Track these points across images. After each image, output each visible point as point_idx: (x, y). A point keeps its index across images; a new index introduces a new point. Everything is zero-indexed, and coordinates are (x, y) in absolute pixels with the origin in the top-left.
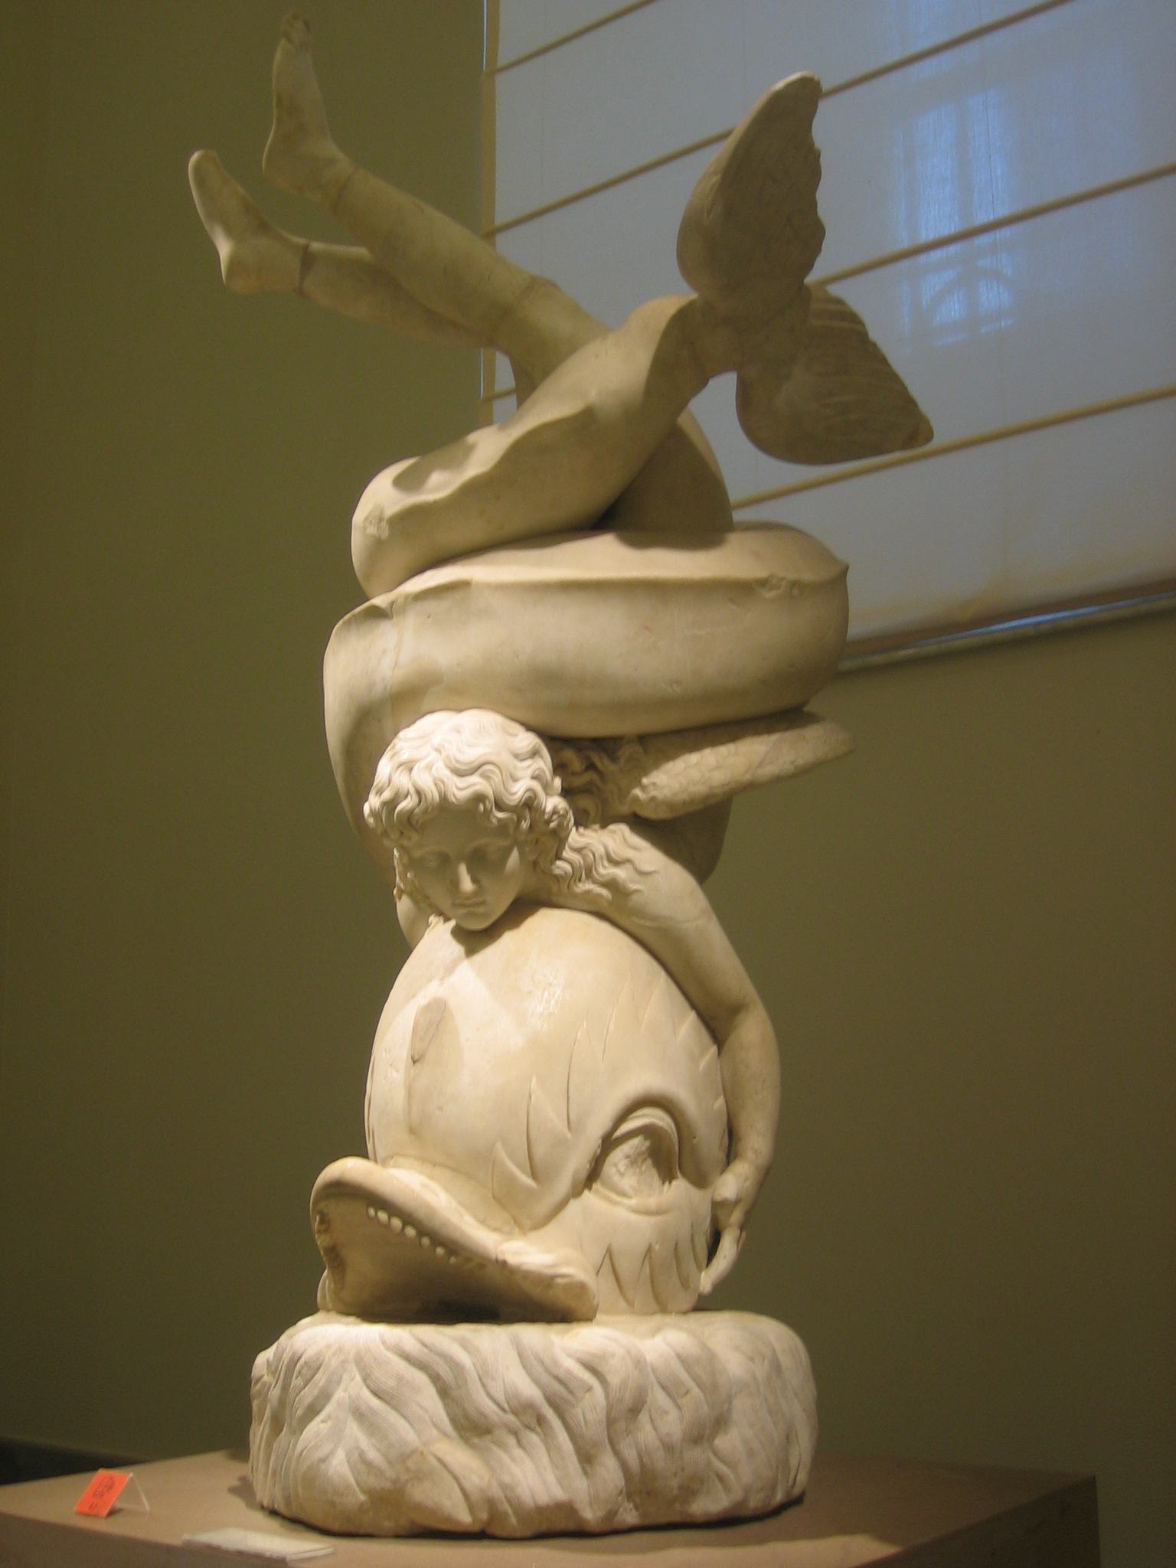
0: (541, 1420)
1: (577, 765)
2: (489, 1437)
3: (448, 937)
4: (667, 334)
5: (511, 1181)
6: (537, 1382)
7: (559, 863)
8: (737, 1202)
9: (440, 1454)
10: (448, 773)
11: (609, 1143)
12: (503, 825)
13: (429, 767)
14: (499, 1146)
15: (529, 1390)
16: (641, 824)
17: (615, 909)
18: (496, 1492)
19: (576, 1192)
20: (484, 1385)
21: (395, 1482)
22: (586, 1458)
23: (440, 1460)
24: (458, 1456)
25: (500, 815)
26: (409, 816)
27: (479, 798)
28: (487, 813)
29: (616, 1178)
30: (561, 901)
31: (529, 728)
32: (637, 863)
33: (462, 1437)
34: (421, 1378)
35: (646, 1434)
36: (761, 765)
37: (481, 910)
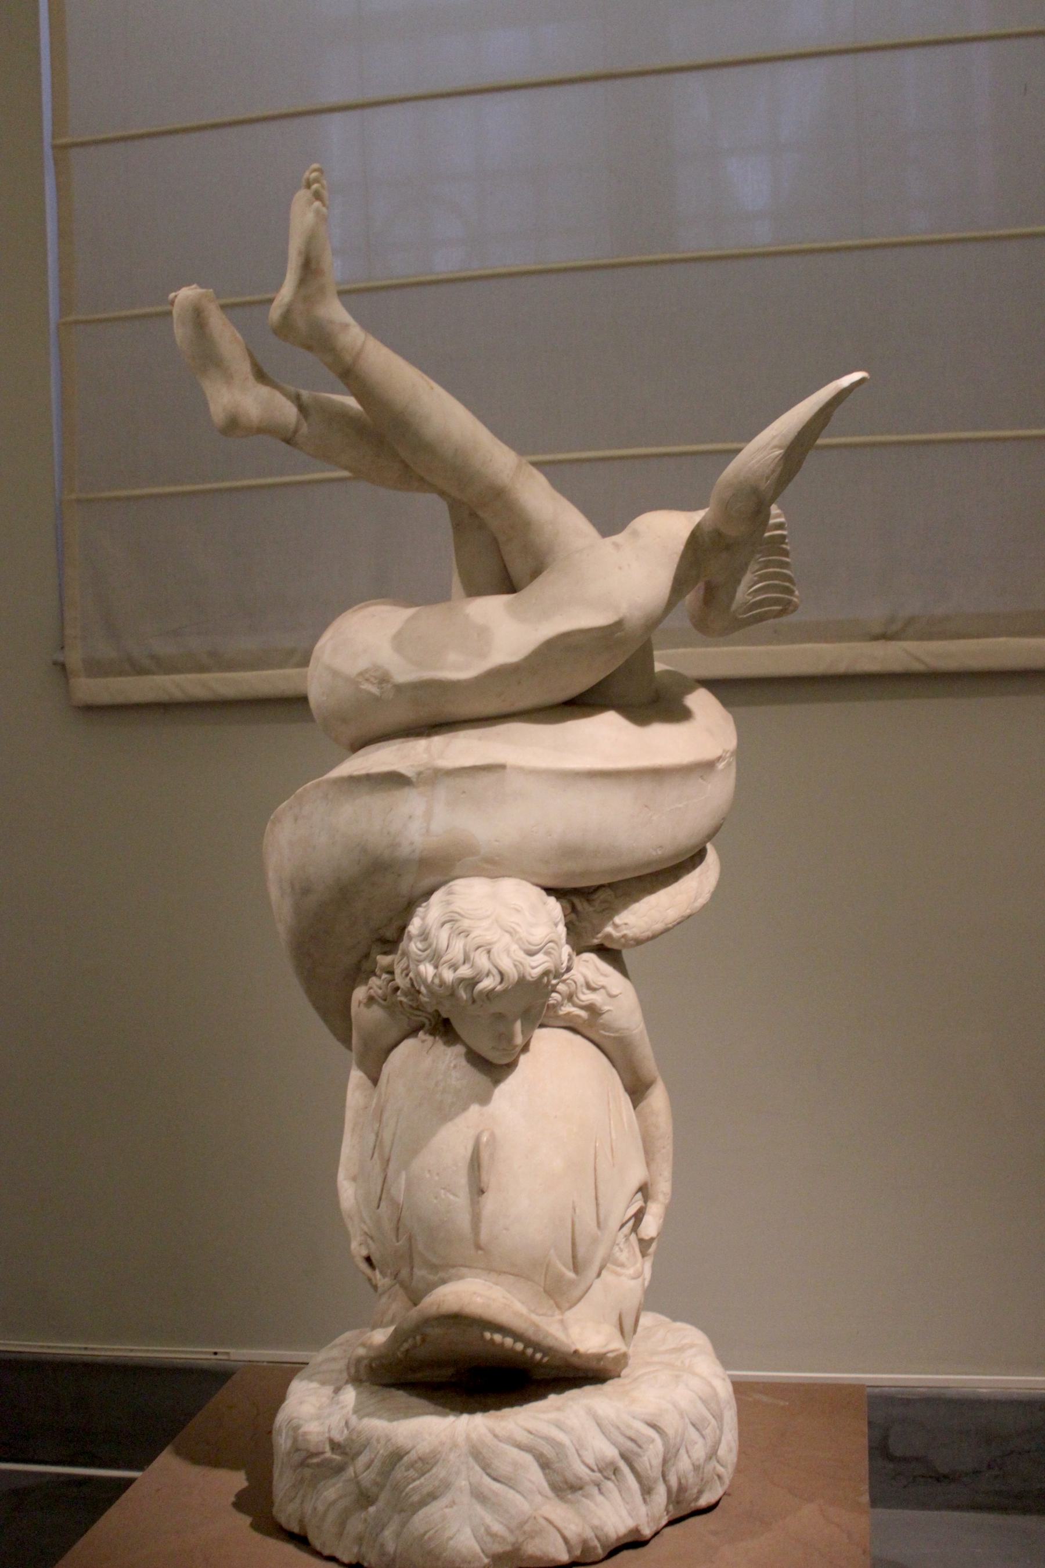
0: (616, 1471)
2: (580, 1492)
4: (683, 556)
5: (561, 1277)
6: (614, 1444)
7: (554, 995)
9: (547, 1515)
10: (522, 954)
13: (508, 952)
14: (552, 1251)
15: (611, 1452)
17: (589, 1027)
18: (589, 1534)
19: (599, 1275)
20: (579, 1456)
21: (513, 1544)
22: (647, 1491)
23: (547, 1519)
24: (557, 1511)
26: (489, 995)
29: (618, 1254)
31: (549, 891)
33: (558, 1496)
34: (528, 1458)
35: (684, 1464)
36: (696, 899)
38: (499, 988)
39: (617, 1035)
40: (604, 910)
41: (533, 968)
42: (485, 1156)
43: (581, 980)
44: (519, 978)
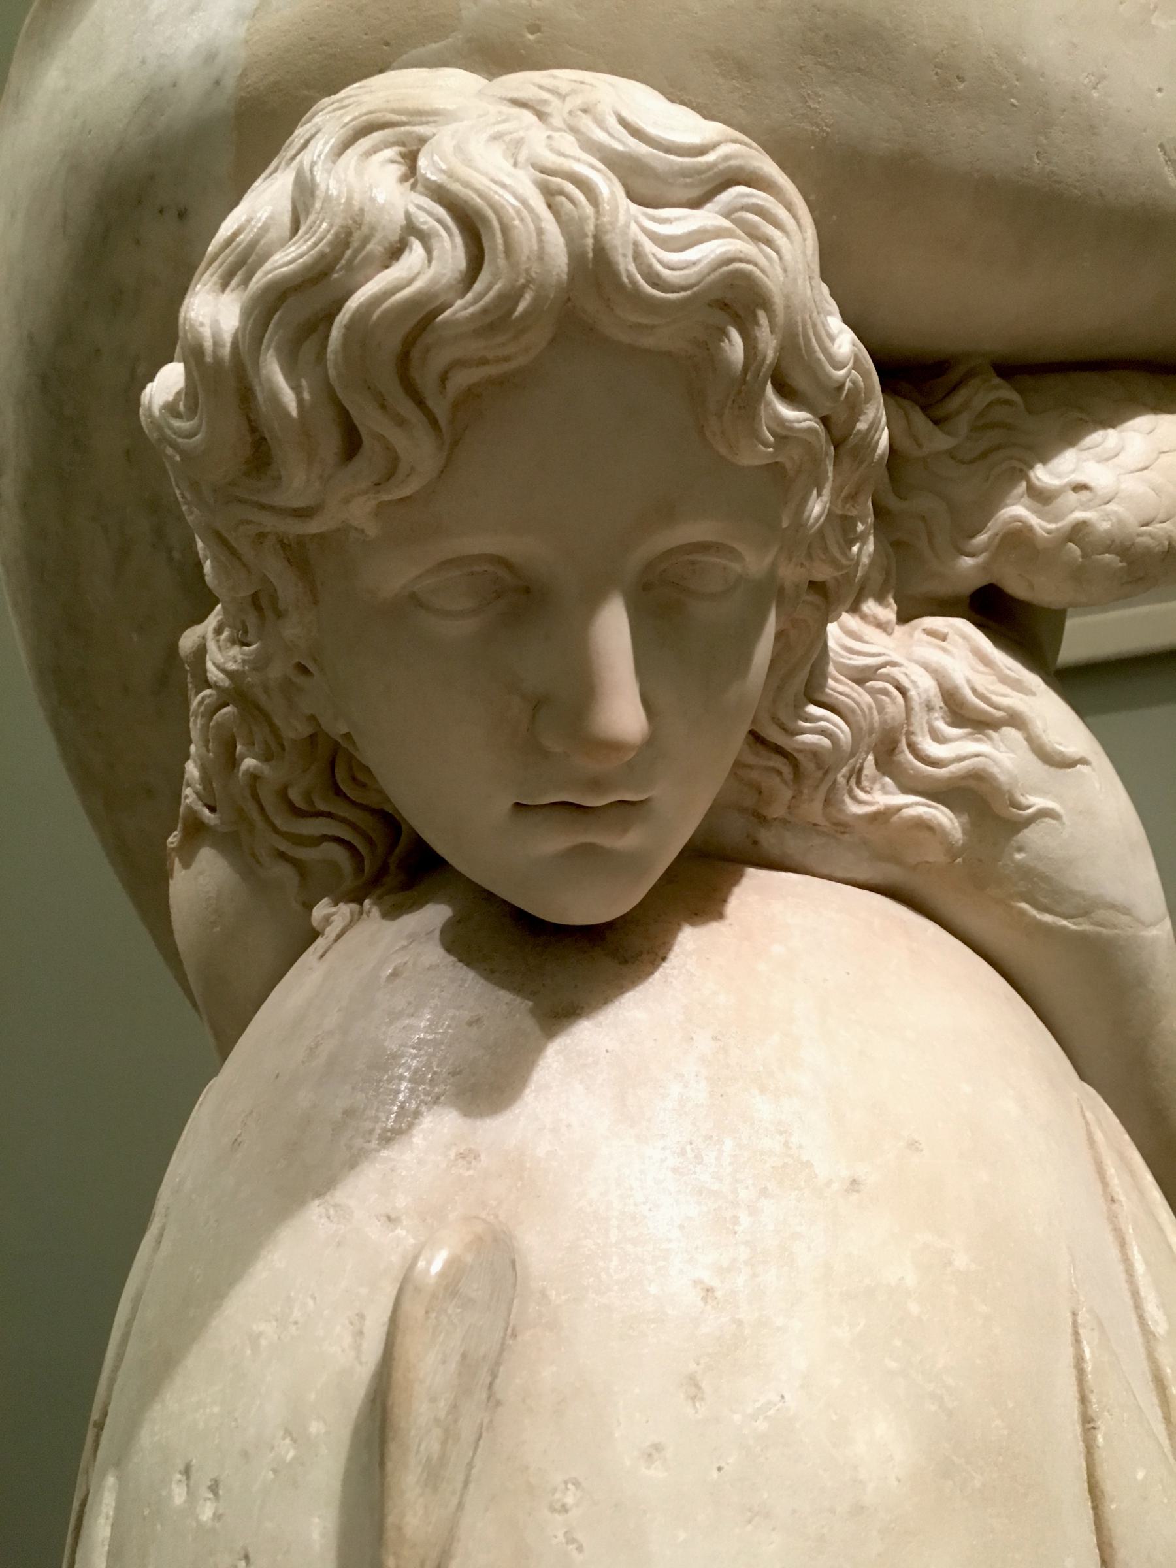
3: (434, 954)
7: (812, 709)
17: (967, 878)
25: (789, 413)
28: (743, 396)
30: (793, 845)
37: (630, 840)
38: (461, 308)
39: (1085, 926)
40: (984, 455)
42: (429, 1371)
43: (923, 685)
44: (576, 258)
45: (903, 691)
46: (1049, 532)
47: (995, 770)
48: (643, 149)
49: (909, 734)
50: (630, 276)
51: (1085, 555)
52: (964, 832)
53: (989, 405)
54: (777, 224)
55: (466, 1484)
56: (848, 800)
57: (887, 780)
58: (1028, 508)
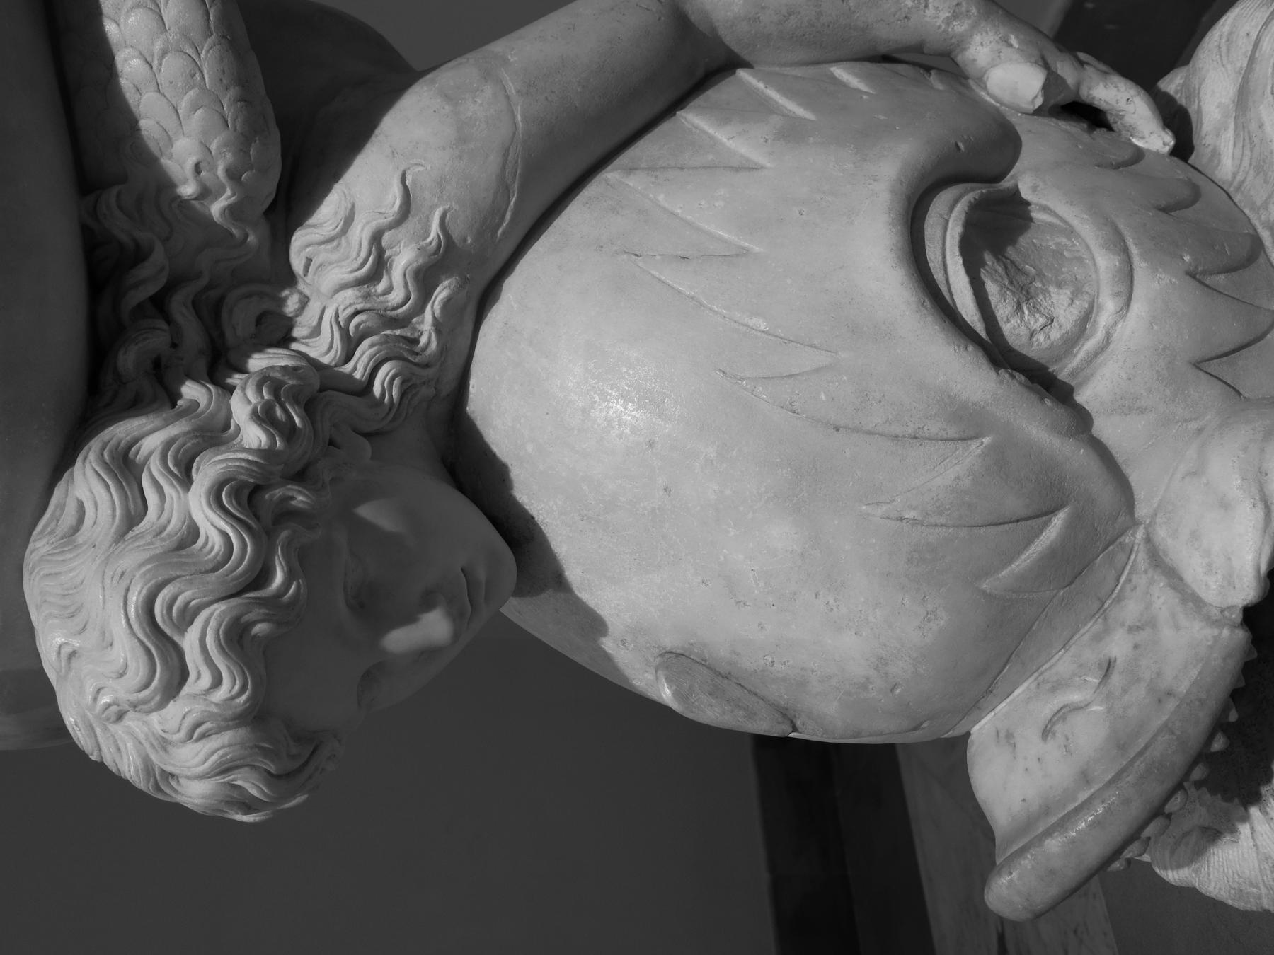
1: (156, 340)
5: (1053, 556)
7: (377, 389)
8: (1046, 66)
11: (998, 353)
12: (300, 565)
13: (164, 744)
16: (291, 200)
19: (1081, 421)
25: (279, 578)
27: (236, 638)
29: (1055, 334)
30: (451, 376)
32: (382, 221)
41: (217, 682)
44: (237, 726)
45: (357, 313)
46: (234, 194)
47: (415, 265)
48: (155, 683)
49: (386, 310)
50: (245, 702)
51: (251, 168)
52: (450, 277)
53: (120, 208)
54: (174, 599)
55: (756, 694)
56: (428, 352)
57: (414, 320)
58: (212, 202)
